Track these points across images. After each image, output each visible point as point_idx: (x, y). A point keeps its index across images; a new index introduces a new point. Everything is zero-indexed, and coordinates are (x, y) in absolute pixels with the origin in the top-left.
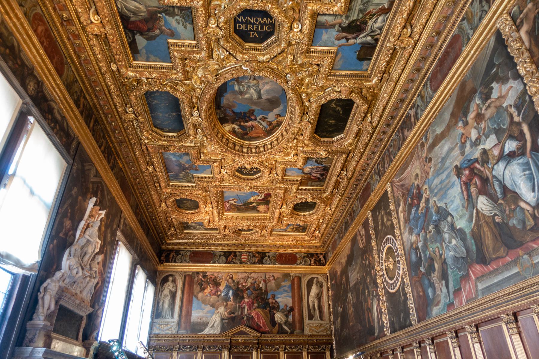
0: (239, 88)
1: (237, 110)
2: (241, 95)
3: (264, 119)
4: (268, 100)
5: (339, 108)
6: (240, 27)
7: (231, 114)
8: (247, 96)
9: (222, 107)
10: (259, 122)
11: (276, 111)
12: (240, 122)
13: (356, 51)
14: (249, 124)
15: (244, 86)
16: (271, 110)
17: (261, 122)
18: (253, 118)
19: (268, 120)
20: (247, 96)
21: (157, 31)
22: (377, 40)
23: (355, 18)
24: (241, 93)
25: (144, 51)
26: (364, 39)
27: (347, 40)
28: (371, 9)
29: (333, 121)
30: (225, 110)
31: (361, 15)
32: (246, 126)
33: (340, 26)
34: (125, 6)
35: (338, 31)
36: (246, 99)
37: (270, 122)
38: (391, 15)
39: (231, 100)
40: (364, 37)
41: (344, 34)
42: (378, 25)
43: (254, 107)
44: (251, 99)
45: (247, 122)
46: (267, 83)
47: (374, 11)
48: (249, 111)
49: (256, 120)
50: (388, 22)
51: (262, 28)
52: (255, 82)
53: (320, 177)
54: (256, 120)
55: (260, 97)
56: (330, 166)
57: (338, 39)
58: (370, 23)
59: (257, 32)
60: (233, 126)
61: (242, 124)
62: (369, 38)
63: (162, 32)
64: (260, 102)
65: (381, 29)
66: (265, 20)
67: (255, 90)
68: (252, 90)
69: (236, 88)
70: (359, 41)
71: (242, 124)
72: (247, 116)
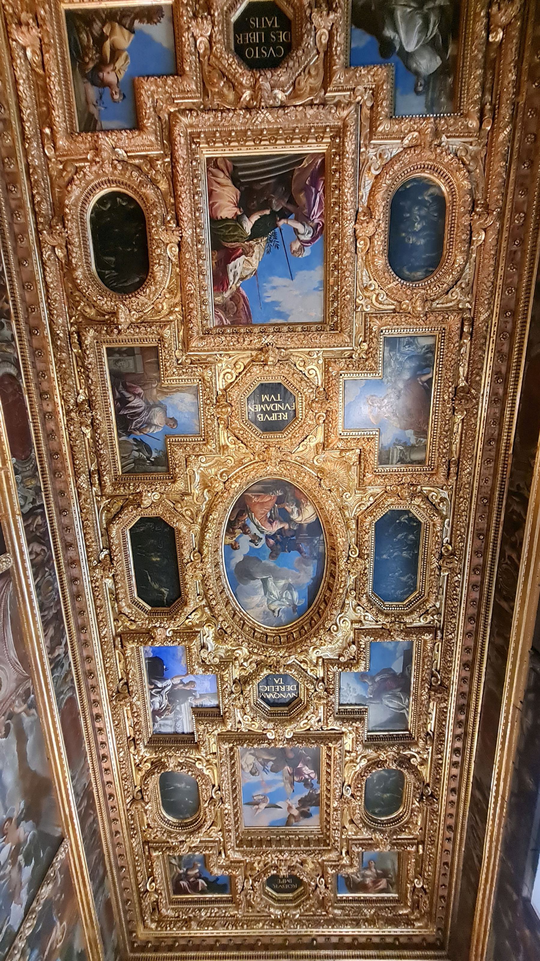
0: (292, 595)
1: (295, 555)
2: (290, 584)
3: (255, 539)
4: (254, 579)
5: (156, 586)
6: (293, 688)
7: (303, 546)
8: (282, 583)
9: (315, 558)
10: (262, 532)
11: (238, 557)
12: (290, 529)
13: (166, 669)
14: (277, 526)
15: (287, 598)
16: (246, 557)
17: (258, 533)
18: (271, 541)
19: (247, 538)
20: (282, 583)
21: (377, 679)
22: (151, 683)
23: (183, 705)
24: (289, 587)
25: (397, 655)
26: (164, 684)
27: (181, 682)
28: (171, 715)
29: (154, 559)
30: (311, 553)
31: (178, 708)
32: (281, 522)
33: (195, 696)
34: (401, 702)
35: (195, 691)
36: (283, 578)
37: (246, 533)
38: (150, 711)
39: (302, 574)
40: (165, 687)
41: (187, 688)
42: (157, 699)
43: (271, 563)
44: (276, 579)
45: (281, 531)
46: (258, 606)
47: (166, 713)
48: (277, 554)
49: (267, 537)
50: (148, 705)
51: (271, 688)
52: (273, 608)
53: (127, 395)
54: (267, 537)
55: (265, 581)
56: (119, 436)
57: (191, 682)
58: (166, 702)
59: (275, 684)
60: (300, 519)
61: (287, 526)
62: (160, 685)
63: (373, 679)
64: (264, 573)
65: (152, 696)
66: (269, 697)
67: (271, 594)
68: (276, 593)
69: (296, 595)
70: (169, 682)
71: (287, 526)
72: (281, 544)
